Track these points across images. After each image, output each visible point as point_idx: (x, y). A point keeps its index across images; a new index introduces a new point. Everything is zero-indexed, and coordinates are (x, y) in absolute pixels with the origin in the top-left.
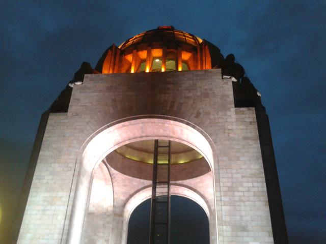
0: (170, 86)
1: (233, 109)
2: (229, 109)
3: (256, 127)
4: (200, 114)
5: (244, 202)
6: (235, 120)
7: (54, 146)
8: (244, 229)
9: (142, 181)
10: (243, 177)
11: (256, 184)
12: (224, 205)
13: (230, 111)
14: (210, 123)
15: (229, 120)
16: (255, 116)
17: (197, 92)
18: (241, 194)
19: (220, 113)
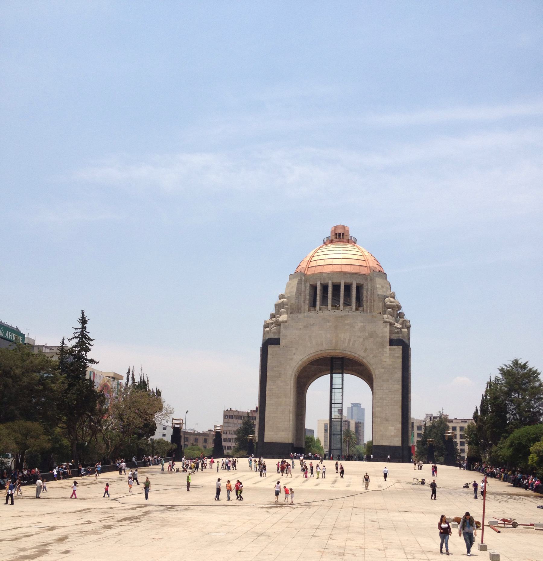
0: (347, 327)
1: (388, 347)
2: (386, 347)
3: (401, 360)
4: (367, 349)
5: (388, 406)
6: (388, 355)
7: (275, 369)
8: (387, 420)
9: (319, 367)
10: (390, 392)
11: (396, 396)
12: (377, 407)
13: (386, 348)
14: (373, 356)
15: (385, 354)
16: (401, 352)
17: (365, 333)
18: (387, 401)
19: (380, 350)
